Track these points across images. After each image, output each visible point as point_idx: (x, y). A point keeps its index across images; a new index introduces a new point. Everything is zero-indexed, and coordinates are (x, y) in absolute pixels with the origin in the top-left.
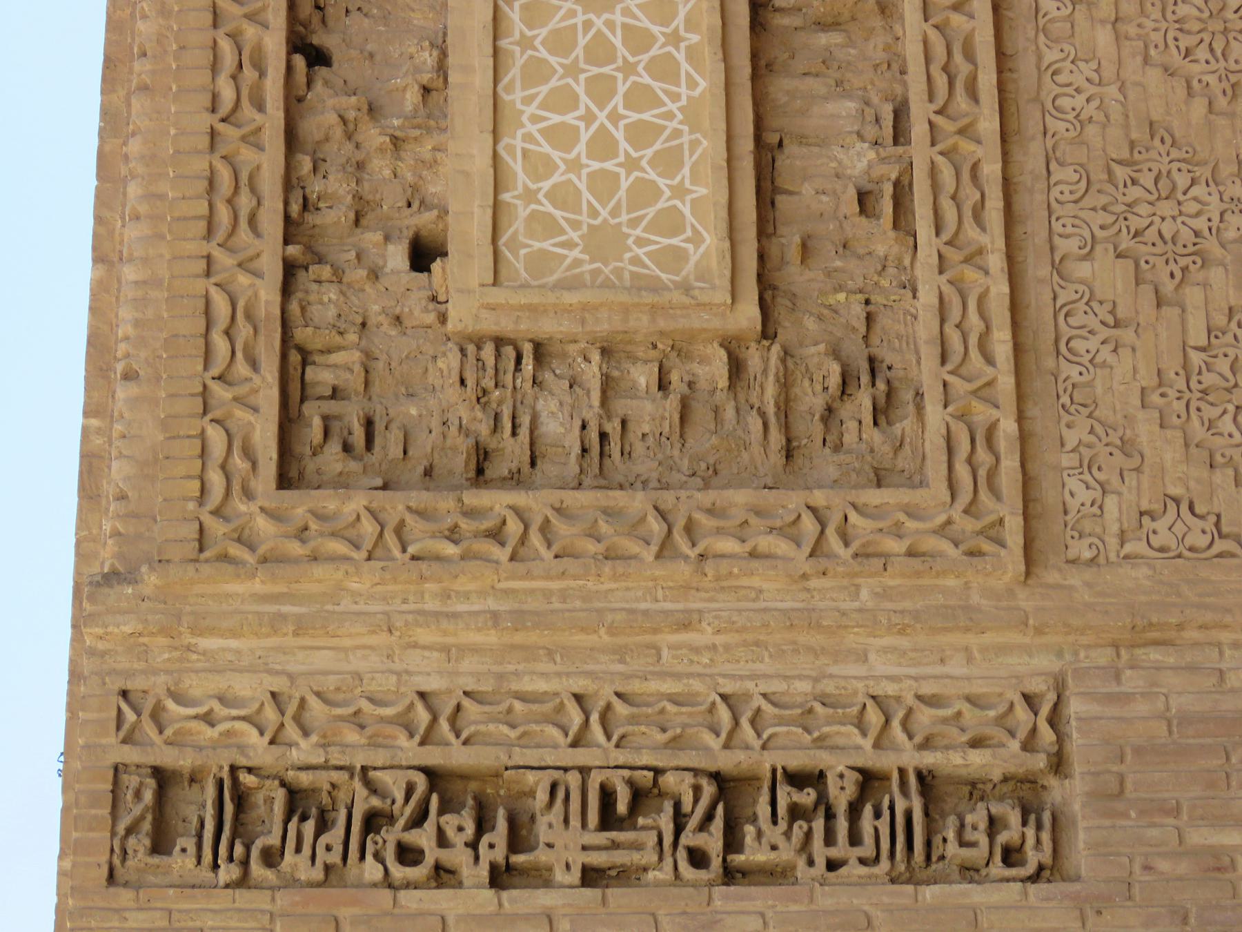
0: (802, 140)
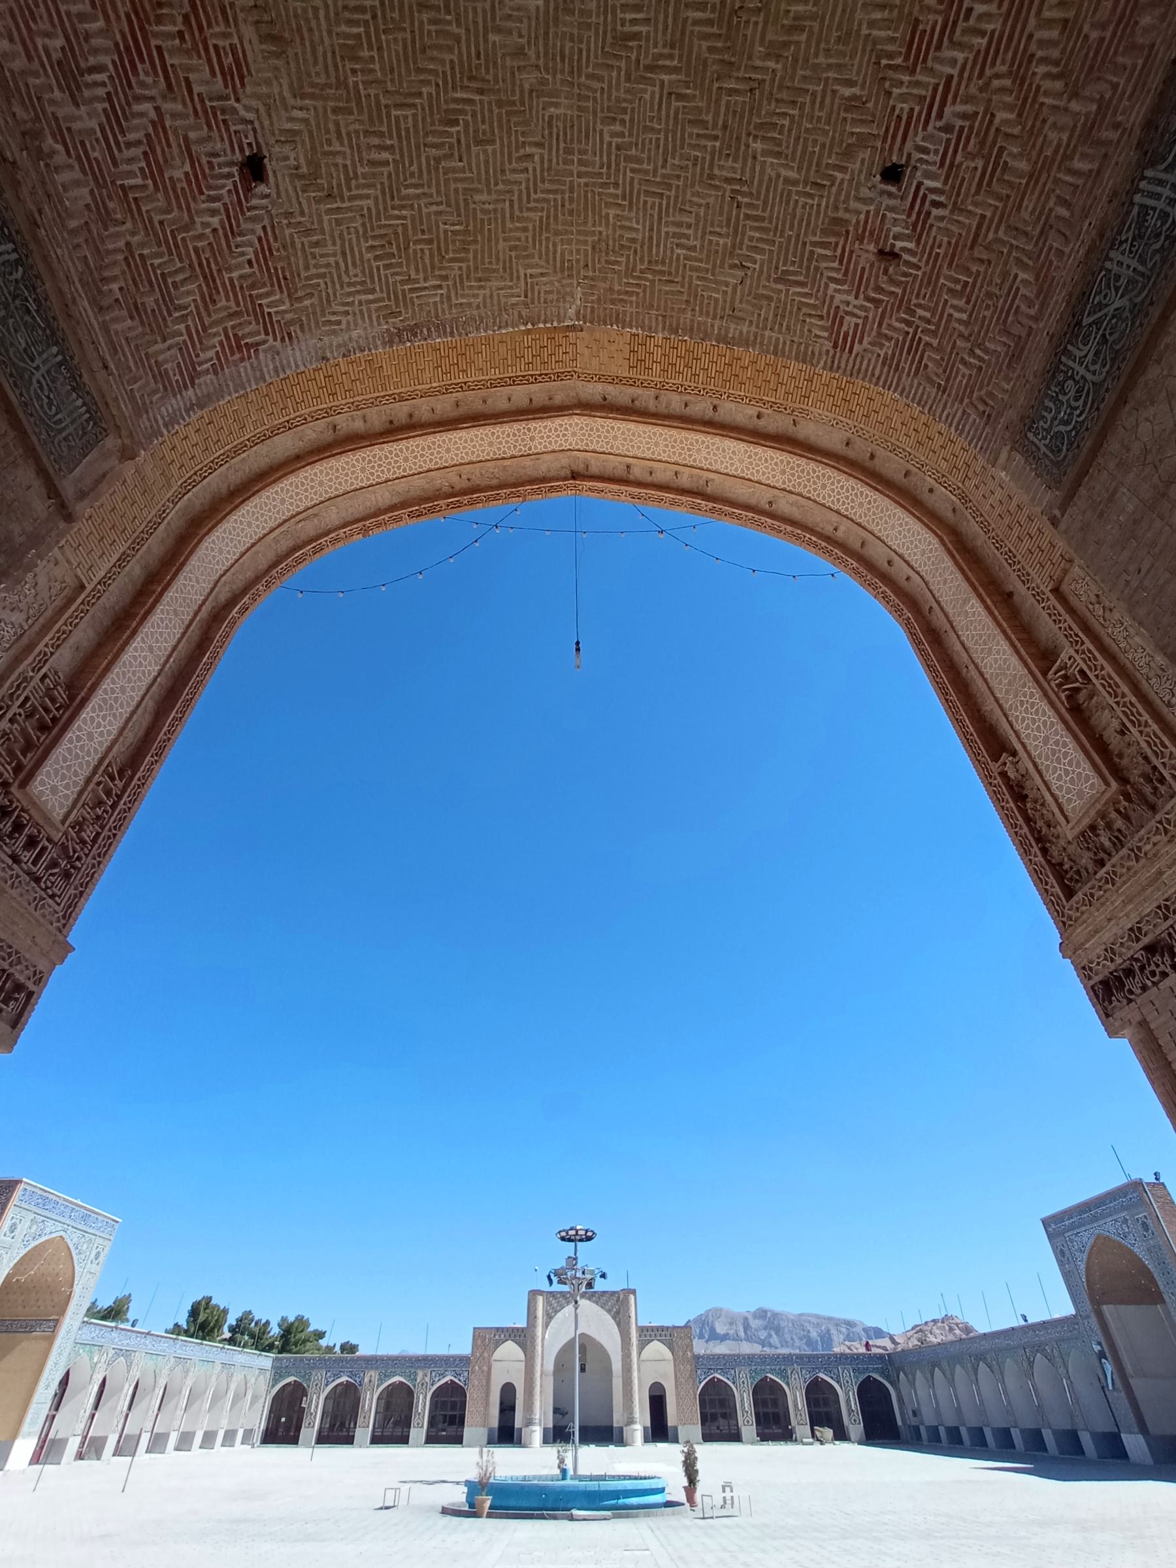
0: (1104, 729)
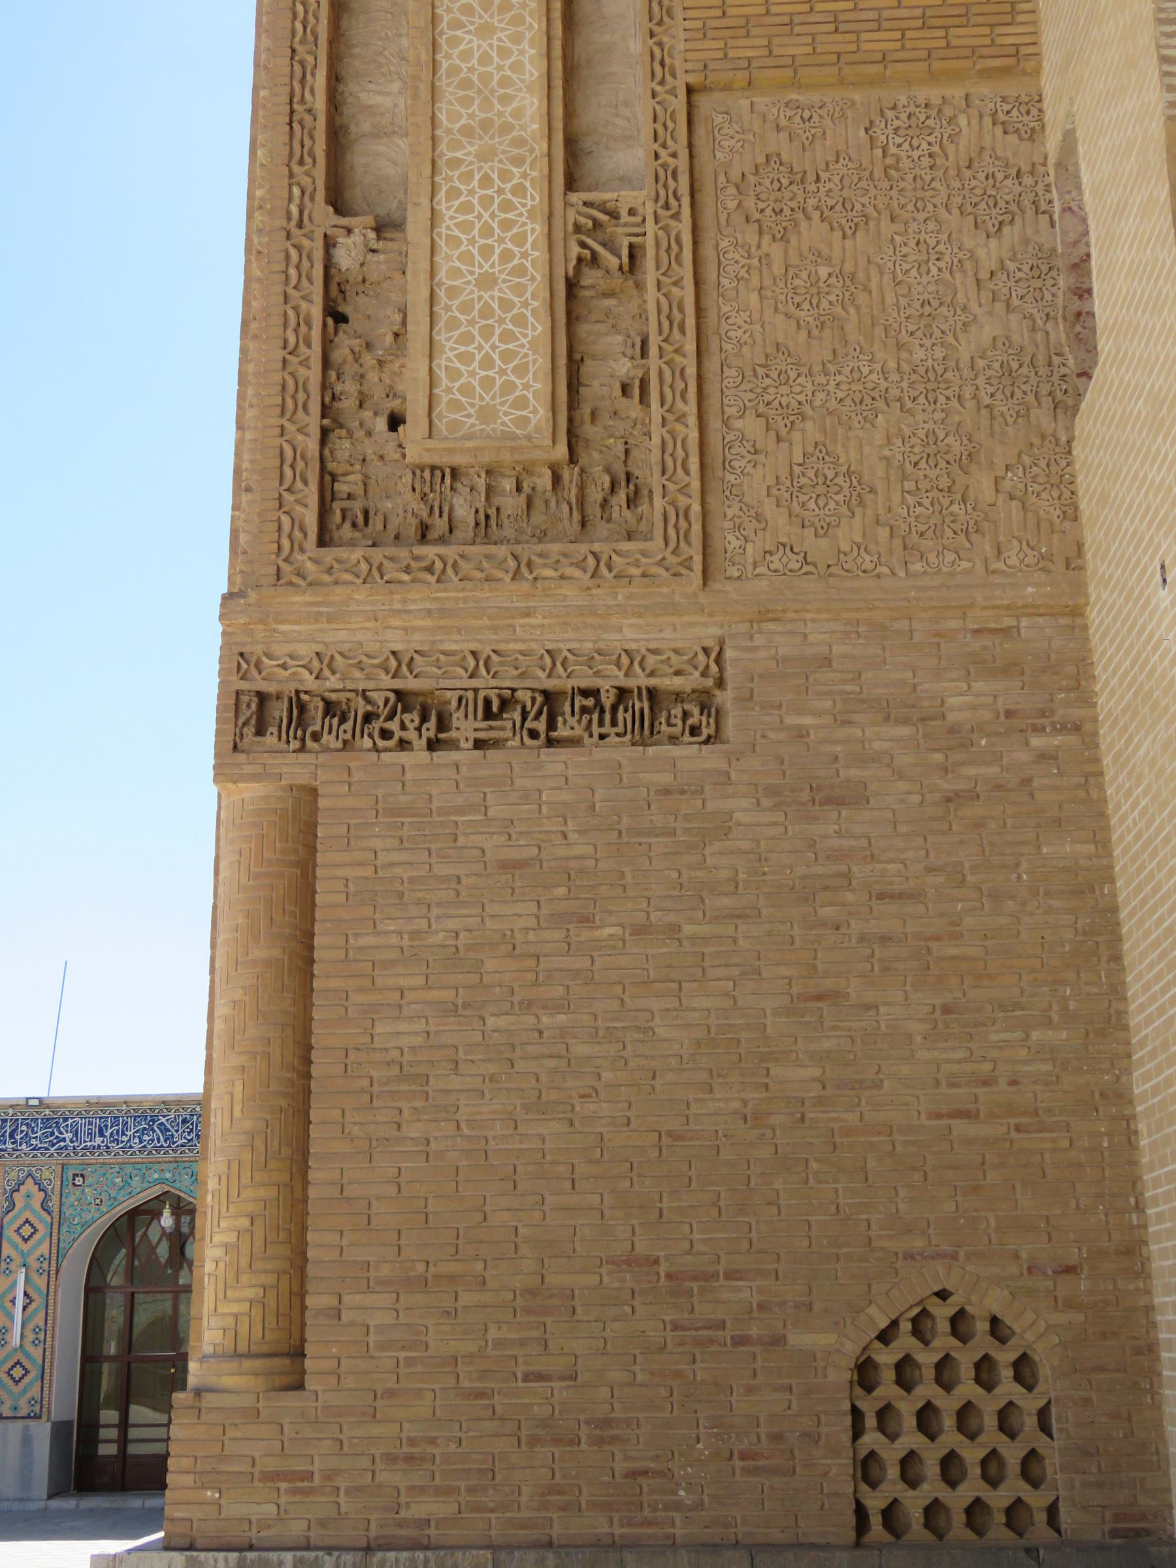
0: (594, 357)
